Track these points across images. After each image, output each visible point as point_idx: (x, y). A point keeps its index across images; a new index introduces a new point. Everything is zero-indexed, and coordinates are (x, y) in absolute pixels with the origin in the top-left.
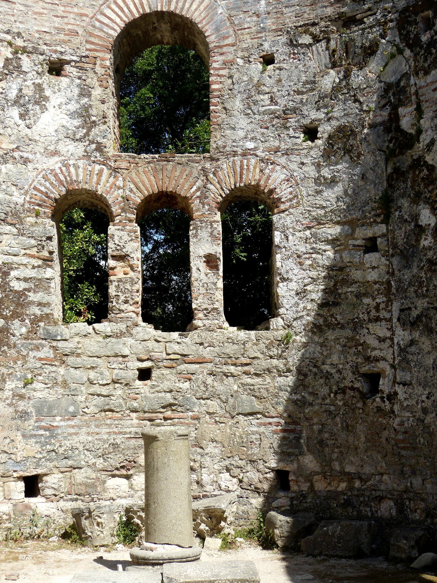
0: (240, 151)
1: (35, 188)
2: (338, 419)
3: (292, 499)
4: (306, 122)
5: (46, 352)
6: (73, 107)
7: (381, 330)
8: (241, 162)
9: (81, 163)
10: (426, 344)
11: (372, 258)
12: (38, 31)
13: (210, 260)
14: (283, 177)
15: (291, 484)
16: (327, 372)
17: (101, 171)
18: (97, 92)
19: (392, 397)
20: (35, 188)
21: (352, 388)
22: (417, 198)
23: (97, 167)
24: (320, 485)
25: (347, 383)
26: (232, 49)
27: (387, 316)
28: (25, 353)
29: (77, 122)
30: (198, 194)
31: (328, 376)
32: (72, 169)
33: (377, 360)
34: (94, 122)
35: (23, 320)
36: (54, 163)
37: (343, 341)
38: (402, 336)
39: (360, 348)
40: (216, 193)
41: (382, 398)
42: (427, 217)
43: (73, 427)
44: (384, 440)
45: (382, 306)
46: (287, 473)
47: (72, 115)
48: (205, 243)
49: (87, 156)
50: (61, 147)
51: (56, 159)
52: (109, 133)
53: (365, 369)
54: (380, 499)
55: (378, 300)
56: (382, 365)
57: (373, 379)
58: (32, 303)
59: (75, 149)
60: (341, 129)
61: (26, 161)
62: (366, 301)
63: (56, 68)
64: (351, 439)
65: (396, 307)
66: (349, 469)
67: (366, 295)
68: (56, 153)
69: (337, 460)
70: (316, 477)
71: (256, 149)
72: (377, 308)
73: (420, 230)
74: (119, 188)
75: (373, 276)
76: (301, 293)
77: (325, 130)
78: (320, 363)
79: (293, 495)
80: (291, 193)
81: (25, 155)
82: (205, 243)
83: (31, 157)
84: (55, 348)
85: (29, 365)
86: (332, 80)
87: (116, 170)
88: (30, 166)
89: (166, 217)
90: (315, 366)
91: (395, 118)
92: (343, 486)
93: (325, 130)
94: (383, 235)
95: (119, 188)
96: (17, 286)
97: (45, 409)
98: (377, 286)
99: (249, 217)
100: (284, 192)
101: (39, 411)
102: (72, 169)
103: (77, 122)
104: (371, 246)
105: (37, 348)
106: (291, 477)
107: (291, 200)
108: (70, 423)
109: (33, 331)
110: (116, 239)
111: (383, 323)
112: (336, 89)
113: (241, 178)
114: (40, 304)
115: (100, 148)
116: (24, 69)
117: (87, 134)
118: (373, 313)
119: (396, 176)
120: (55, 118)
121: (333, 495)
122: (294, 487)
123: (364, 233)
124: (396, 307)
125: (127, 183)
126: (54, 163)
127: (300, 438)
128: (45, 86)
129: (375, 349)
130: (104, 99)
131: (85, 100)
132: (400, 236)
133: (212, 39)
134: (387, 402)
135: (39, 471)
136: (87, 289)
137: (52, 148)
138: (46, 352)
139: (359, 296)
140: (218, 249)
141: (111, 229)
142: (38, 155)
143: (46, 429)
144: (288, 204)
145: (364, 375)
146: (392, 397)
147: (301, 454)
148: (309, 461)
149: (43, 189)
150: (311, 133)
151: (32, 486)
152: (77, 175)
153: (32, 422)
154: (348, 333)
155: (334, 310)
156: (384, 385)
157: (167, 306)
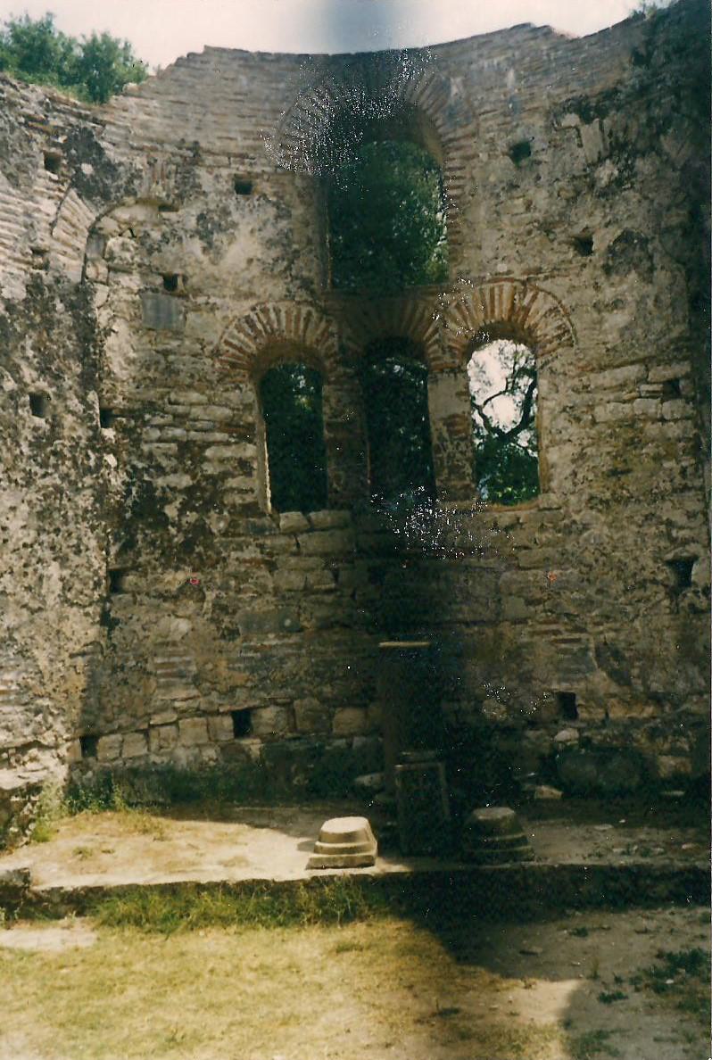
0: (488, 276)
1: (227, 343)
2: (637, 623)
3: (580, 730)
4: (577, 230)
5: (251, 553)
6: (270, 232)
8: (492, 290)
9: (283, 307)
12: (220, 138)
14: (547, 307)
15: (579, 710)
16: (620, 561)
17: (309, 314)
20: (227, 343)
21: (654, 582)
23: (305, 310)
24: (617, 713)
25: (646, 574)
26: (471, 142)
27: (698, 483)
28: (224, 554)
29: (275, 252)
30: (437, 336)
31: (621, 567)
32: (273, 316)
33: (685, 542)
34: (296, 251)
35: (221, 512)
37: (639, 519)
39: (663, 528)
41: (696, 593)
43: (290, 646)
44: (702, 649)
45: (689, 471)
46: (573, 696)
49: (289, 296)
50: (259, 290)
51: (252, 302)
53: (670, 556)
55: (684, 464)
56: (693, 548)
58: (232, 489)
60: (626, 237)
61: (213, 308)
62: (667, 465)
64: (657, 648)
66: (655, 686)
67: (668, 456)
68: (249, 295)
69: (639, 677)
70: (613, 700)
71: (509, 272)
72: (683, 472)
74: (332, 335)
75: (674, 430)
77: (601, 242)
78: (609, 549)
79: (583, 725)
80: (559, 328)
81: (212, 300)
83: (219, 301)
84: (261, 546)
85: (231, 569)
86: (608, 172)
88: (219, 314)
90: (603, 554)
92: (649, 710)
93: (601, 242)
94: (687, 376)
95: (332, 335)
96: (210, 469)
98: (681, 444)
101: (248, 626)
102: (273, 316)
103: (275, 252)
105: (240, 548)
106: (579, 701)
107: (559, 337)
108: (286, 640)
109: (233, 524)
110: (333, 401)
111: (692, 493)
112: (618, 182)
113: (493, 311)
114: (241, 491)
116: (204, 188)
117: (288, 268)
118: (678, 480)
121: (634, 723)
122: (583, 714)
123: (662, 373)
127: (587, 649)
128: (232, 208)
129: (682, 528)
131: (283, 224)
134: (703, 598)
135: (251, 704)
137: (245, 288)
138: (251, 553)
139: (657, 458)
142: (227, 299)
143: (256, 650)
144: (556, 342)
145: (670, 563)
147: (592, 670)
149: (235, 342)
150: (583, 245)
151: (243, 723)
152: (279, 321)
153: (238, 641)
154: (646, 509)
155: (623, 478)
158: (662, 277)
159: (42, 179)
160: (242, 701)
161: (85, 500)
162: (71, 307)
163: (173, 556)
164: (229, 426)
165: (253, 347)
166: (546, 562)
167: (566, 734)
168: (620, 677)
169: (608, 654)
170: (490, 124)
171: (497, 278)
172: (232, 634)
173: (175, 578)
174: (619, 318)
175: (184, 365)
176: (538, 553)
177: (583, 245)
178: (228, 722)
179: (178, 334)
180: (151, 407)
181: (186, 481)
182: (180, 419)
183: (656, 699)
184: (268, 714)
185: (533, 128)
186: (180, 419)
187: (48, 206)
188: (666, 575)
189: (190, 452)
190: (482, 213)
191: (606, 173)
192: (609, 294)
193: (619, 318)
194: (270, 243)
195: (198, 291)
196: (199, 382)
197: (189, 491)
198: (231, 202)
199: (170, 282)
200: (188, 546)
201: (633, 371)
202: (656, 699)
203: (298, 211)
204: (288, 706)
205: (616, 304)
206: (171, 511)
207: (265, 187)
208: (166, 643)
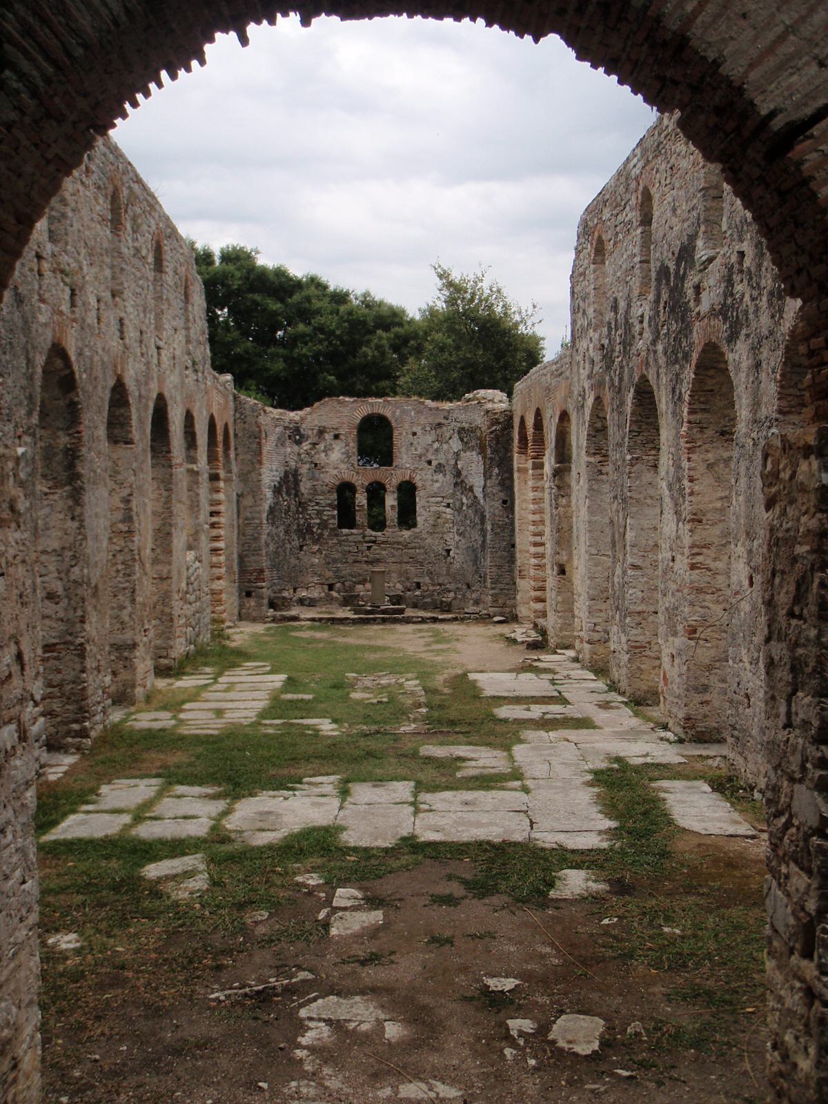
5: (335, 541)
6: (343, 450)
7: (451, 535)
10: (463, 541)
11: (448, 510)
13: (392, 507)
18: (352, 444)
19: (454, 558)
22: (462, 493)
36: (335, 472)
38: (457, 538)
40: (395, 482)
42: (465, 500)
47: (343, 453)
48: (391, 500)
52: (354, 459)
54: (450, 591)
57: (448, 551)
59: (343, 466)
60: (440, 464)
63: (336, 437)
65: (455, 528)
73: (463, 504)
75: (449, 516)
76: (426, 520)
82: (391, 500)
87: (358, 473)
89: (376, 492)
91: (456, 464)
93: (434, 463)
96: (325, 518)
97: (335, 561)
99: (408, 491)
100: (419, 484)
104: (448, 506)
115: (353, 465)
119: (456, 484)
120: (336, 455)
121: (434, 591)
124: (455, 528)
125: (361, 478)
126: (335, 472)
130: (353, 447)
132: (458, 504)
133: (394, 424)
136: (346, 517)
138: (335, 541)
140: (396, 503)
141: (357, 495)
146: (454, 558)
148: (427, 580)
151: (331, 587)
156: (451, 553)
157: (378, 523)
158: (448, 477)
159: (288, 442)
160: (331, 581)
161: (295, 527)
162: (293, 476)
163: (316, 542)
164: (330, 505)
165: (337, 483)
166: (414, 548)
167: (418, 593)
168: (431, 579)
169: (430, 573)
170: (407, 426)
171: (406, 468)
172: (329, 563)
173: (316, 548)
174: (437, 485)
175: (319, 488)
176: (413, 545)
177: (430, 463)
178: (326, 587)
179: (318, 480)
180: (310, 501)
181: (318, 521)
182: (317, 504)
183: (440, 585)
184: (338, 585)
185: (418, 429)
186: (317, 504)
187: (289, 450)
188: (444, 553)
189: (319, 513)
190: (403, 450)
191: (436, 445)
192: (435, 478)
193: (437, 485)
194: (343, 453)
195: (323, 467)
196: (323, 493)
197: (319, 524)
198: (333, 442)
199: (316, 465)
200: (318, 539)
201: (440, 499)
202: (440, 585)
203: (352, 444)
204: (343, 583)
205: (437, 481)
206: (315, 530)
207: (341, 437)
208: (313, 565)
